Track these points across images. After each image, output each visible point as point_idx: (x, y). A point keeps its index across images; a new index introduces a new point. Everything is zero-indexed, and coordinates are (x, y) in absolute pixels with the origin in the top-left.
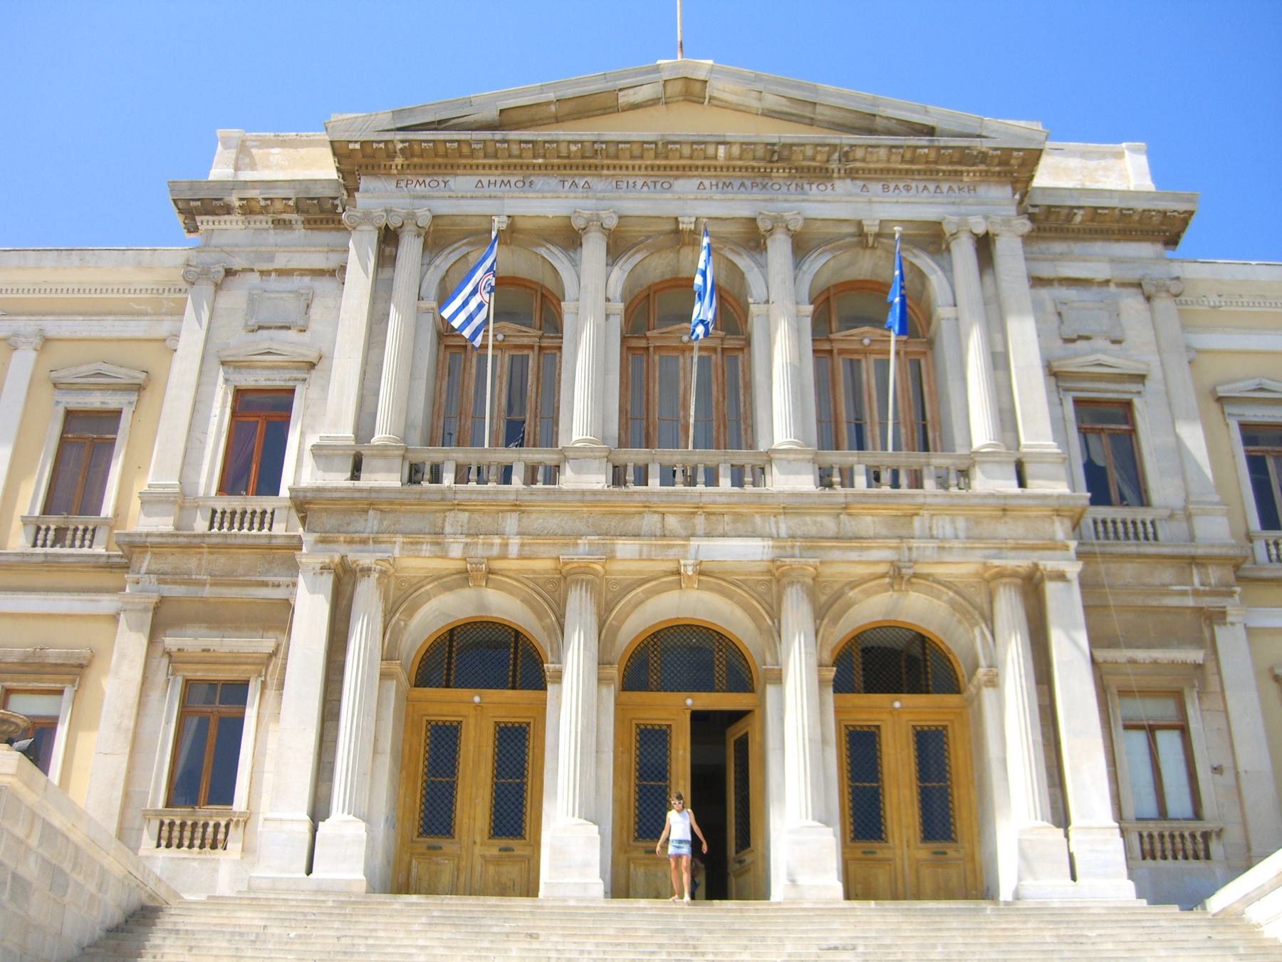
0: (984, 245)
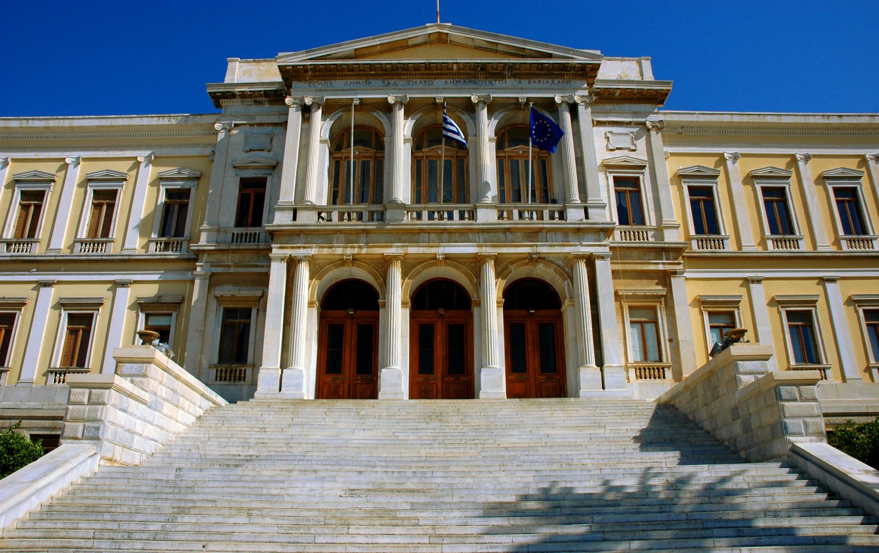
0: (573, 109)
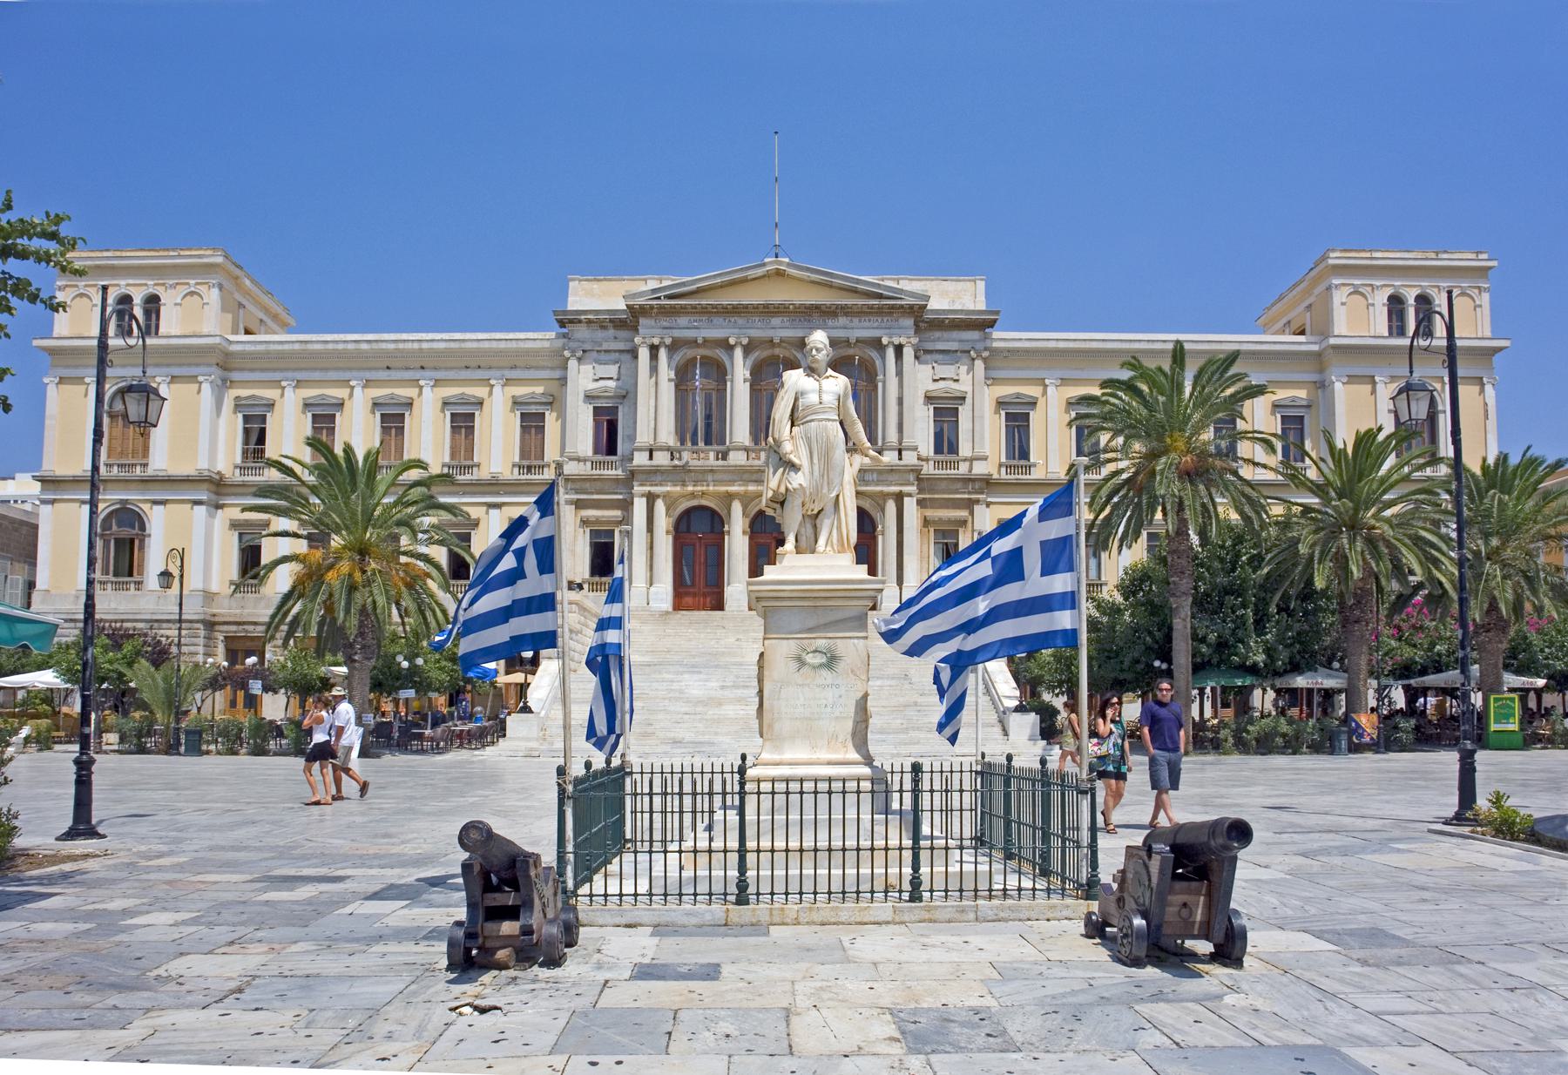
0: (899, 350)
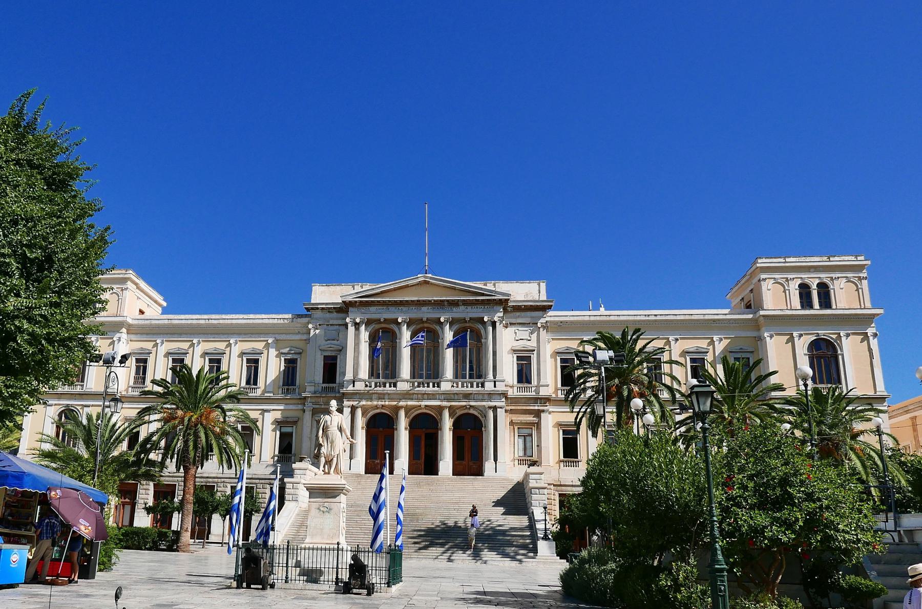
0: (494, 324)
